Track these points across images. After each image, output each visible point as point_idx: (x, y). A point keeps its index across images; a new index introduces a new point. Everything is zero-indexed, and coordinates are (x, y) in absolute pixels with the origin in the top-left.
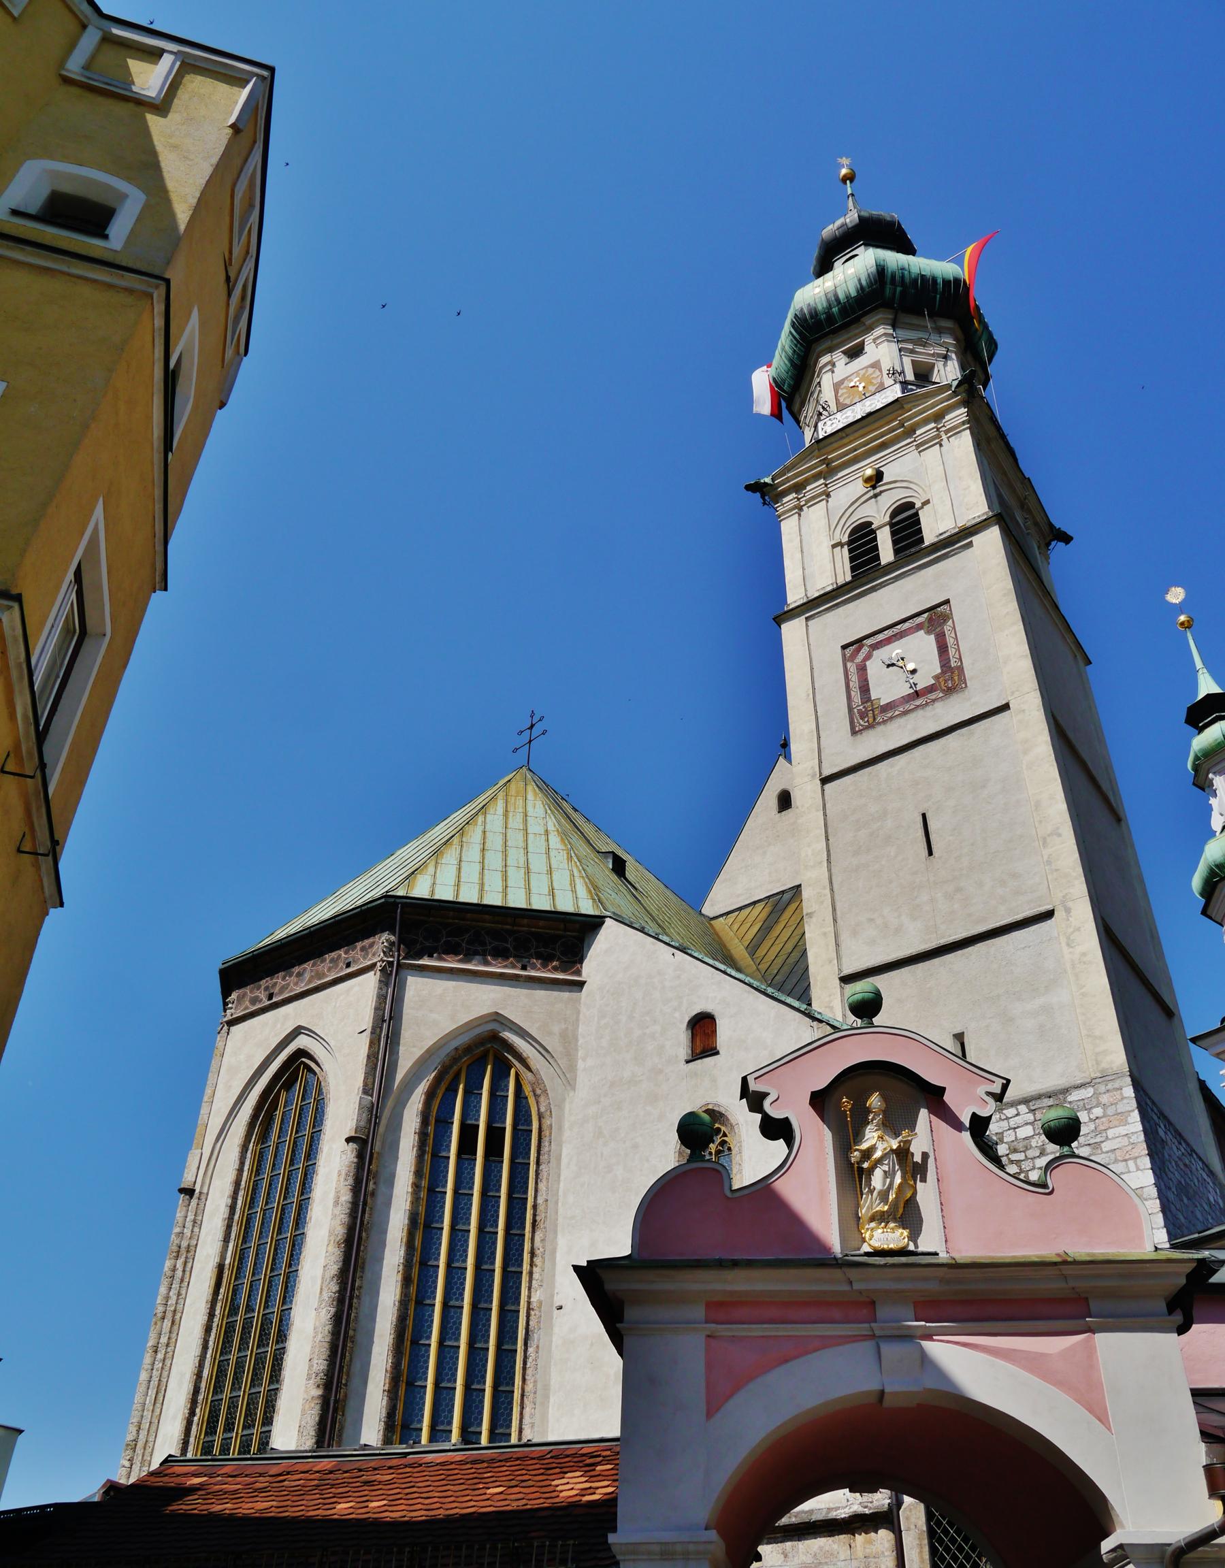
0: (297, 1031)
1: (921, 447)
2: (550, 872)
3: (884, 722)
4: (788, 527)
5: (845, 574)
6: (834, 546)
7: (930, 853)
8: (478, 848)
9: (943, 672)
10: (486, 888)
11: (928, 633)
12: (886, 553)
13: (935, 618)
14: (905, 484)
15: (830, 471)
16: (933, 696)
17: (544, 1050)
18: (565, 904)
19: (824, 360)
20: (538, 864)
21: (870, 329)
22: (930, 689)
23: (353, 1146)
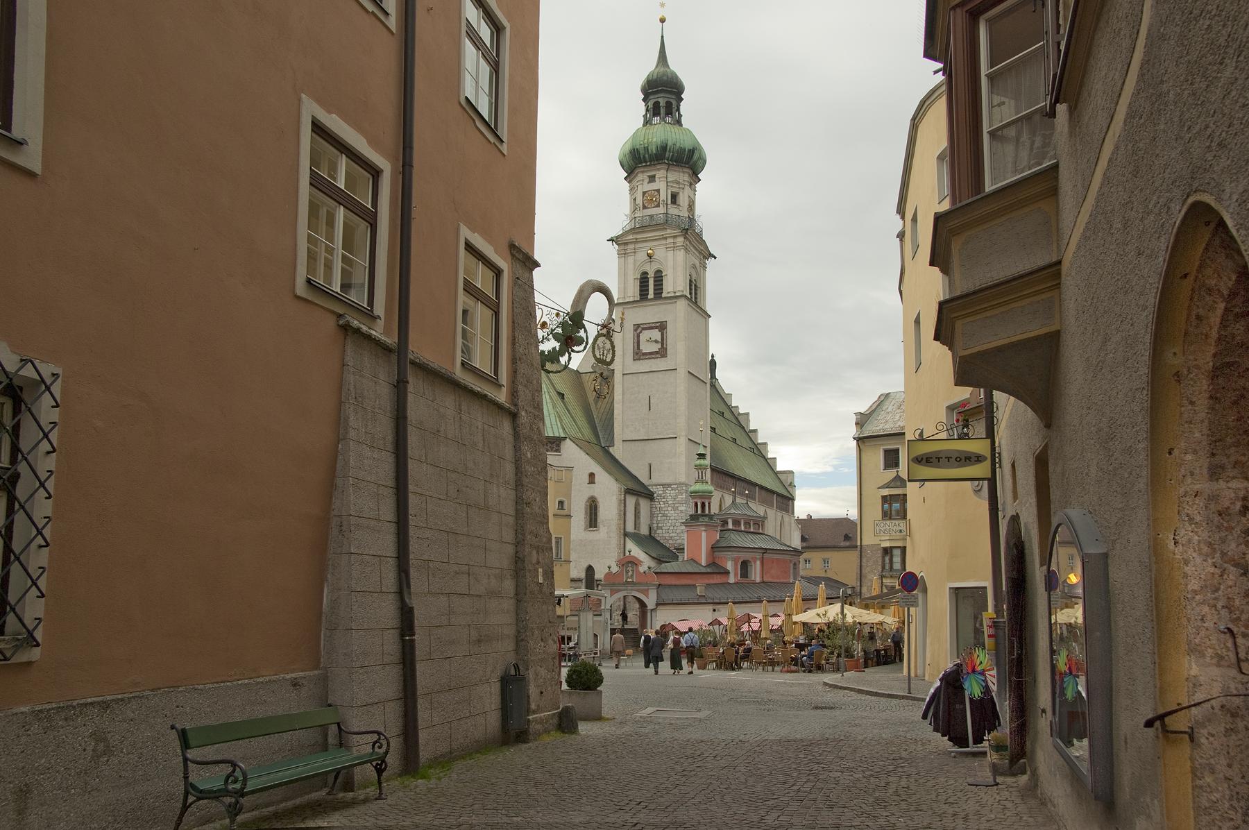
13: (662, 327)
15: (636, 241)
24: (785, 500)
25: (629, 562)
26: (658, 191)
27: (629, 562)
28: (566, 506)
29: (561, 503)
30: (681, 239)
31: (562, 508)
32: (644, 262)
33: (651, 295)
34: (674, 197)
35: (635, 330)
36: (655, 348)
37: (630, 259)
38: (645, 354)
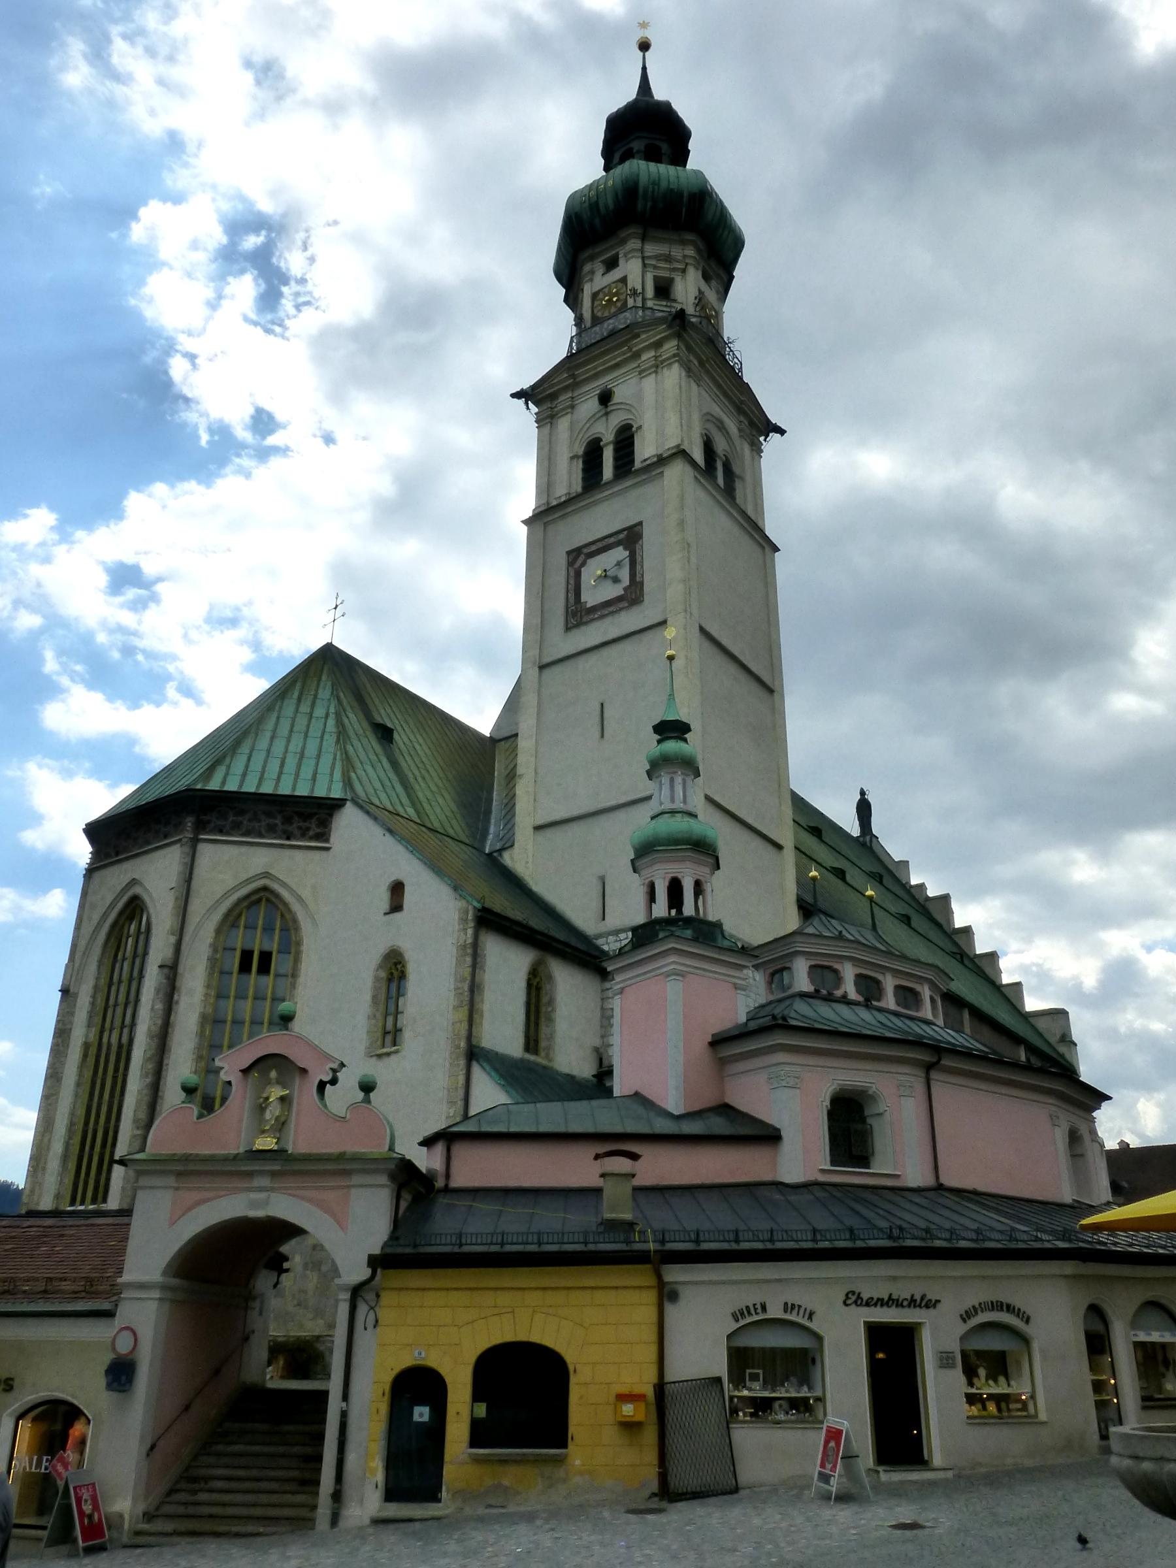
0: (134, 882)
1: (642, 373)
2: (318, 756)
3: (586, 623)
5: (578, 487)
6: (572, 458)
7: (602, 736)
8: (268, 734)
9: (630, 586)
10: (266, 776)
11: (625, 549)
12: (608, 471)
13: (631, 537)
14: (628, 408)
16: (621, 605)
17: (300, 899)
18: (320, 792)
19: (587, 268)
20: (311, 749)
21: (623, 242)
22: (619, 599)
23: (166, 971)
26: (624, 280)
30: (670, 347)
32: (594, 419)
34: (663, 290)
35: (570, 564)
36: (611, 591)
37: (563, 424)
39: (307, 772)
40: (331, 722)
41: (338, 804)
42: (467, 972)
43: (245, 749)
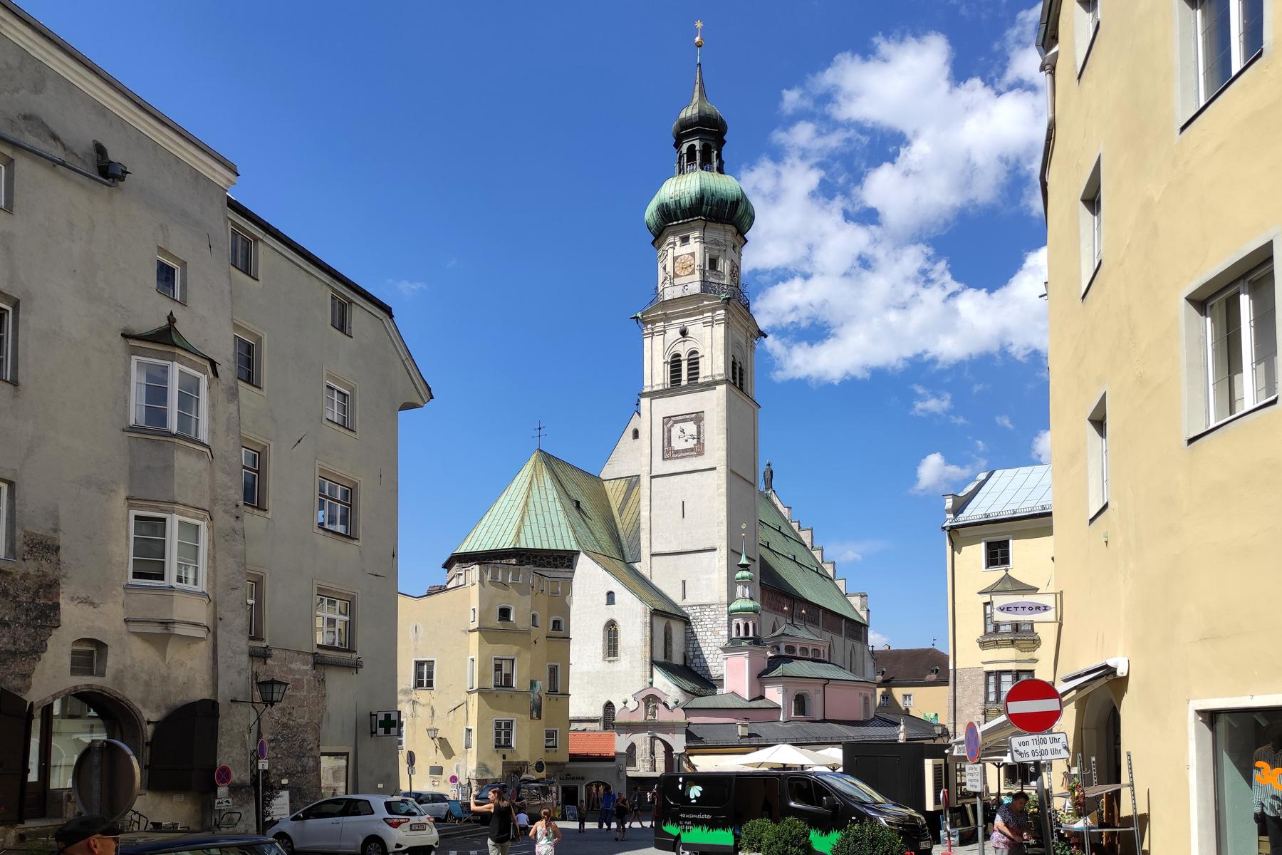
4: (647, 342)
13: (698, 418)
15: (667, 318)
19: (671, 239)
21: (693, 229)
22: (692, 450)
24: (857, 630)
25: (651, 700)
26: (693, 254)
27: (651, 700)
28: (563, 626)
29: (556, 625)
31: (559, 629)
33: (684, 382)
36: (691, 443)
38: (677, 452)
39: (558, 537)
40: (558, 504)
41: (578, 553)
42: (648, 633)
43: (527, 522)
